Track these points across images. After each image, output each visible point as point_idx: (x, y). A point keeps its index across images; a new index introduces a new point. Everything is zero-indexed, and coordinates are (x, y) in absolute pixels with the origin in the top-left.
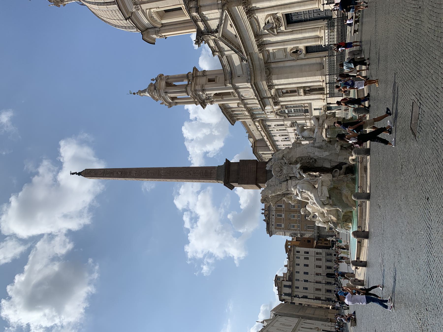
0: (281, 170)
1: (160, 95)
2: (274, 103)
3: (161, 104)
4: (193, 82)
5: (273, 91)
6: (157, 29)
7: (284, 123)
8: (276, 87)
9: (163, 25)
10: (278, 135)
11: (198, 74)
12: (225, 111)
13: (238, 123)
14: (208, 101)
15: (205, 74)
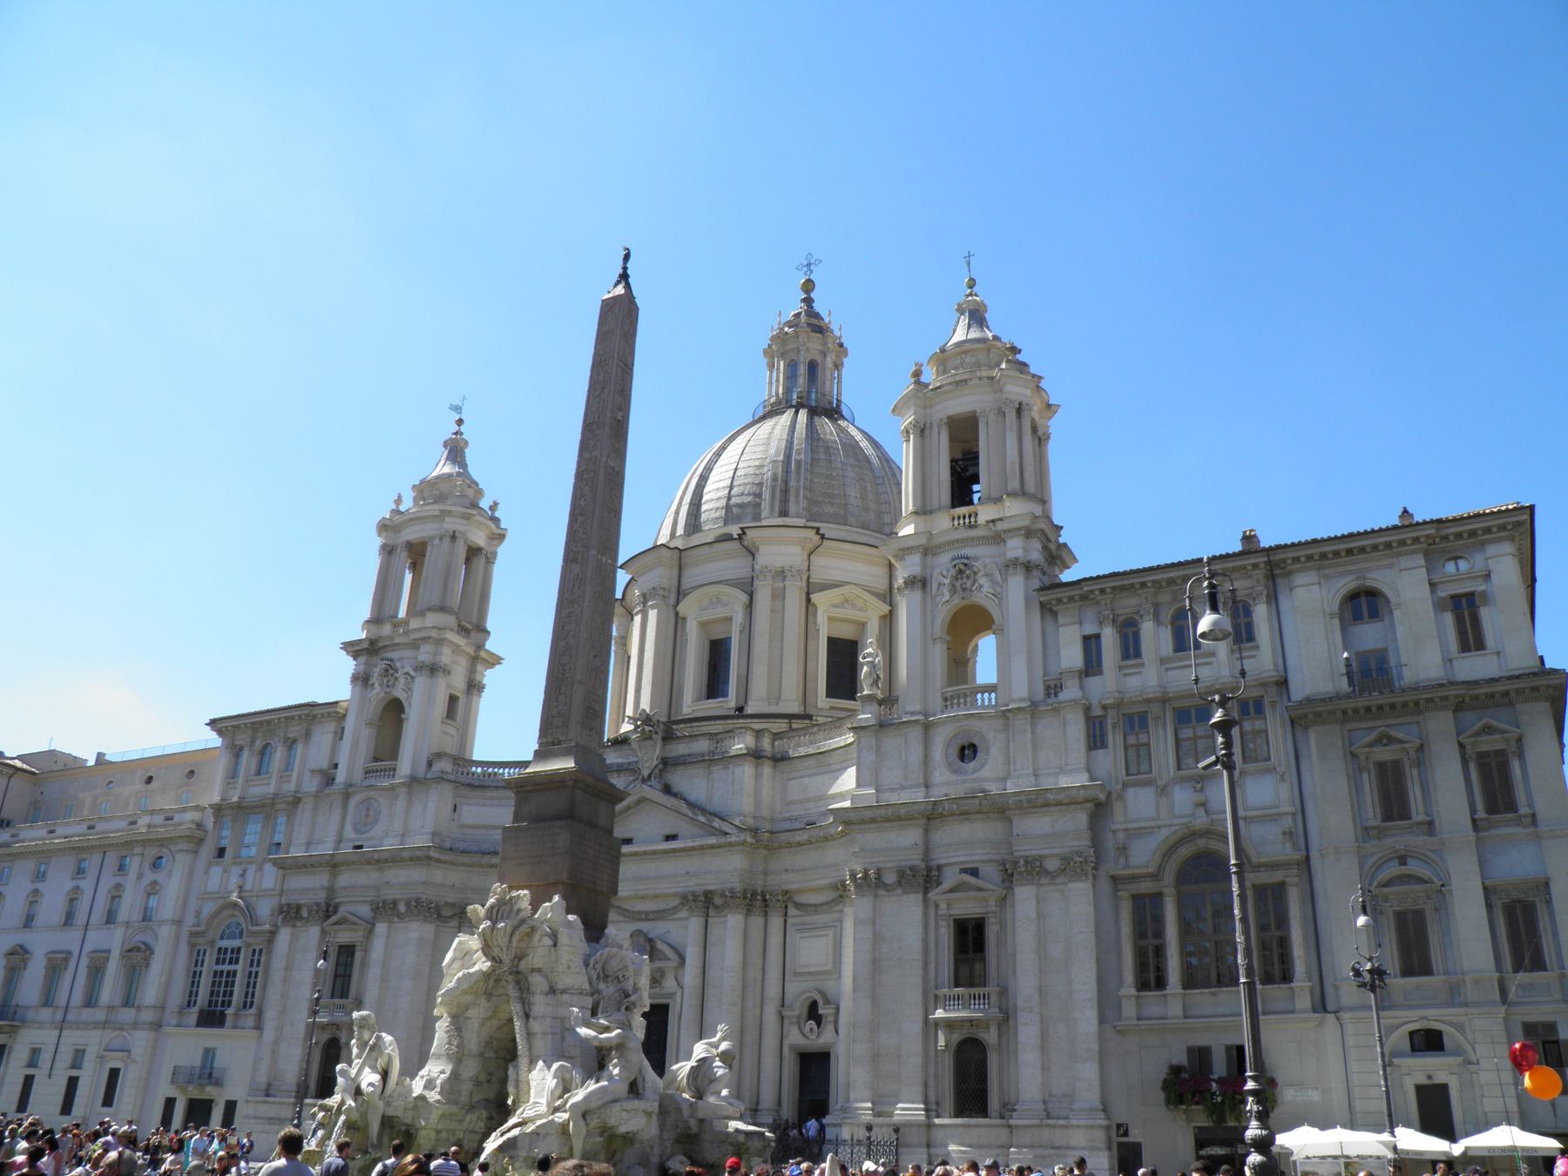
0: (607, 976)
1: (450, 512)
2: (298, 908)
3: (400, 496)
4: (466, 644)
5: (365, 910)
6: (673, 598)
7: (163, 923)
8: (381, 928)
9: (680, 621)
10: (82, 884)
11: (479, 667)
12: (307, 715)
13: (213, 740)
14: (377, 671)
15: (475, 692)
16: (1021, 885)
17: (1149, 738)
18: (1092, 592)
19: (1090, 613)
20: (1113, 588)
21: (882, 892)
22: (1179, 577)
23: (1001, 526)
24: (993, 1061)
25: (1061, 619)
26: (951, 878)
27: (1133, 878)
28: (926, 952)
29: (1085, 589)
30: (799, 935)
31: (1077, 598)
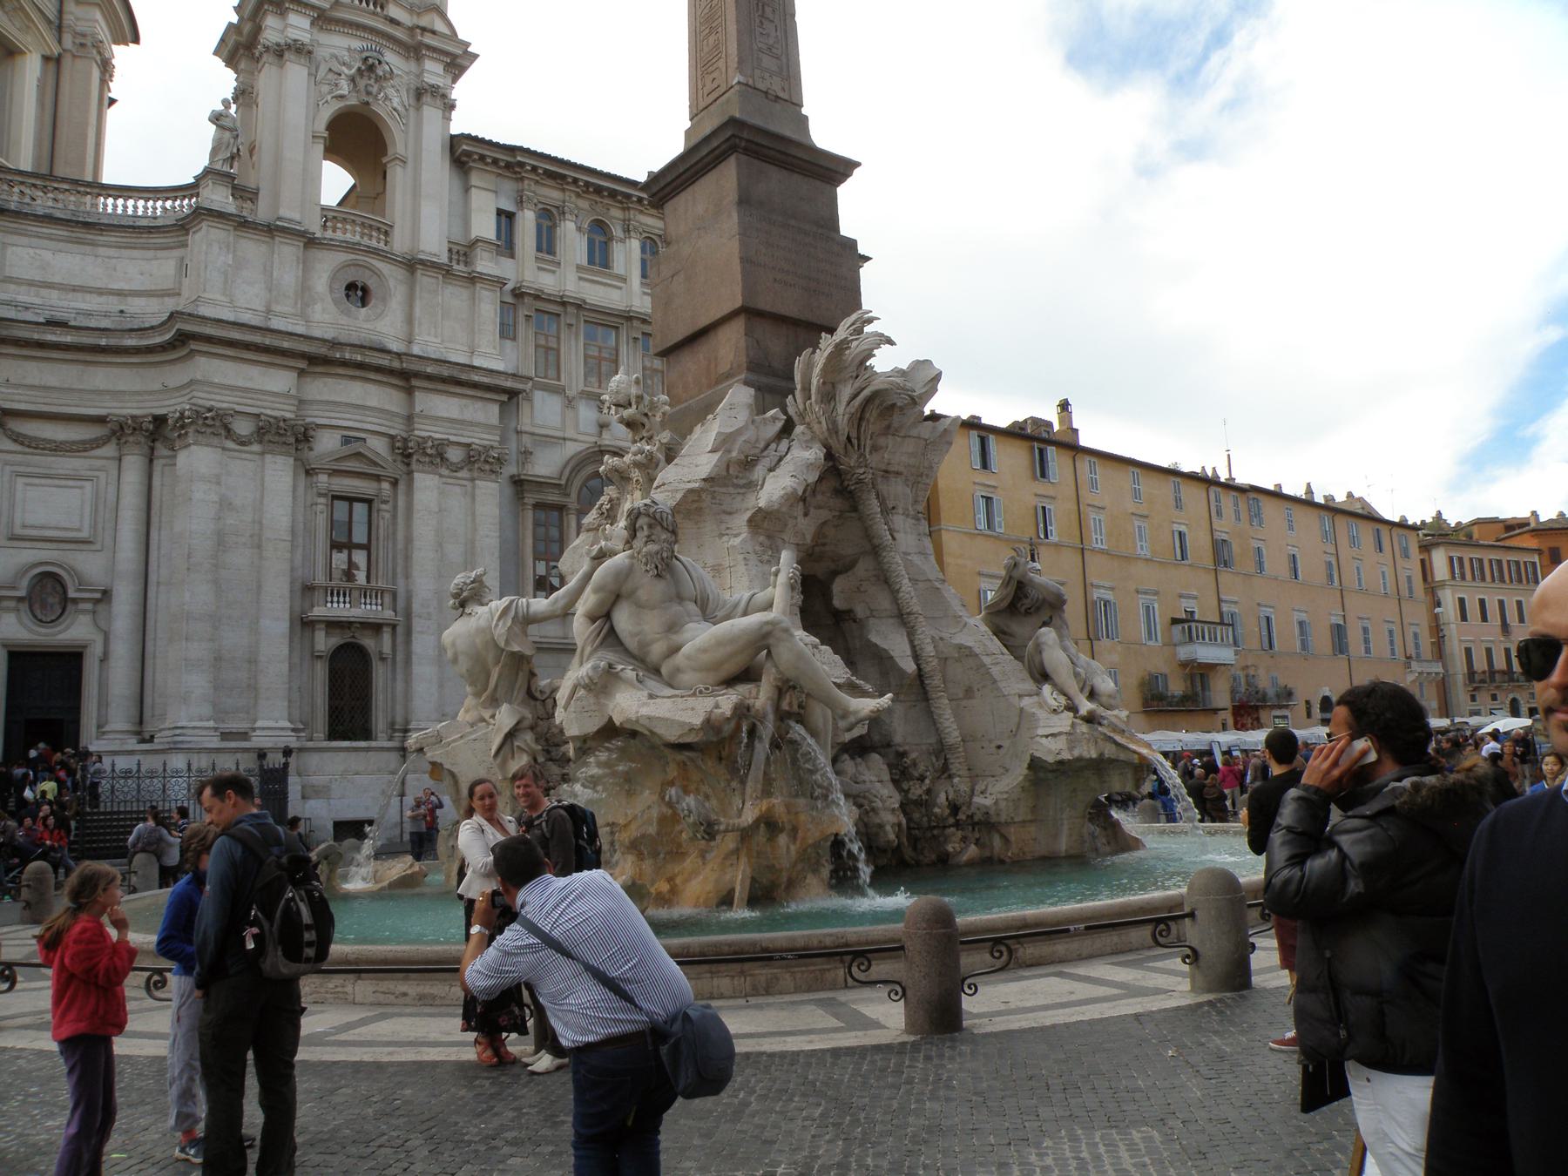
16: (423, 472)
17: (559, 343)
18: (522, 165)
19: (509, 186)
20: (546, 171)
21: (230, 444)
22: (607, 189)
23: (428, 39)
24: (379, 674)
25: (475, 179)
26: (327, 443)
27: (541, 485)
28: (293, 532)
29: (519, 158)
30: (21, 481)
31: (503, 164)
